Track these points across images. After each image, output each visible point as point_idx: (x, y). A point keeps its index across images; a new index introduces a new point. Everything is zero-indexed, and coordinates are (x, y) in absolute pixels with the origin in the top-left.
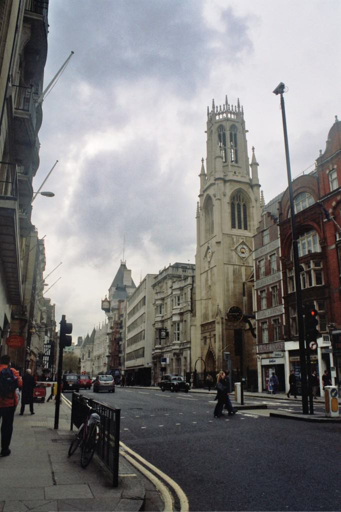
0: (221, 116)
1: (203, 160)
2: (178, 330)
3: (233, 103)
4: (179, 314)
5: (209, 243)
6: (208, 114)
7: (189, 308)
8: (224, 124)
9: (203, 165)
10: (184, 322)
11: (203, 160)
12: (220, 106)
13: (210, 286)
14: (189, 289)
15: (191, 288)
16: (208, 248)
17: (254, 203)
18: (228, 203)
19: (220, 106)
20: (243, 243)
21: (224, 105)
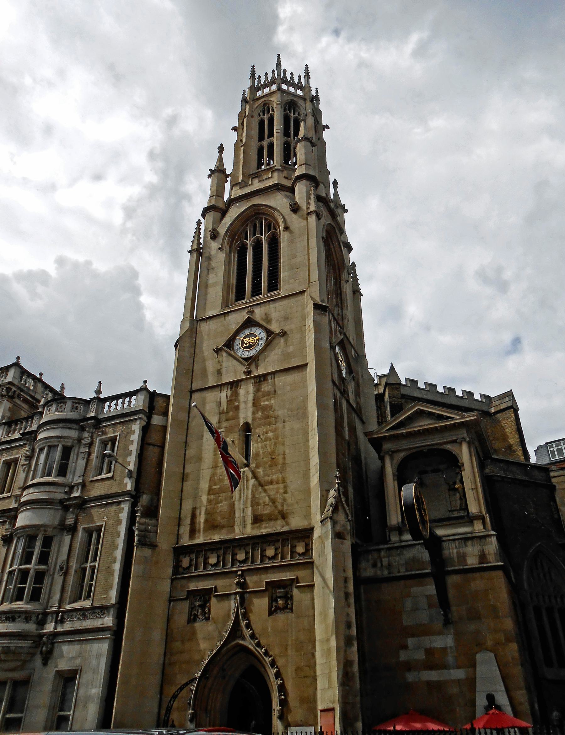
0: (292, 90)
1: (221, 149)
2: (44, 558)
3: (313, 84)
4: (61, 502)
5: (252, 312)
6: (253, 75)
7: (129, 485)
8: (301, 103)
9: (220, 160)
10: (80, 534)
11: (221, 149)
12: (292, 74)
13: (247, 427)
14: (136, 427)
15: (144, 423)
16: (249, 323)
17: (344, 275)
18: (323, 238)
19: (292, 74)
20: (342, 344)
21: (300, 76)
